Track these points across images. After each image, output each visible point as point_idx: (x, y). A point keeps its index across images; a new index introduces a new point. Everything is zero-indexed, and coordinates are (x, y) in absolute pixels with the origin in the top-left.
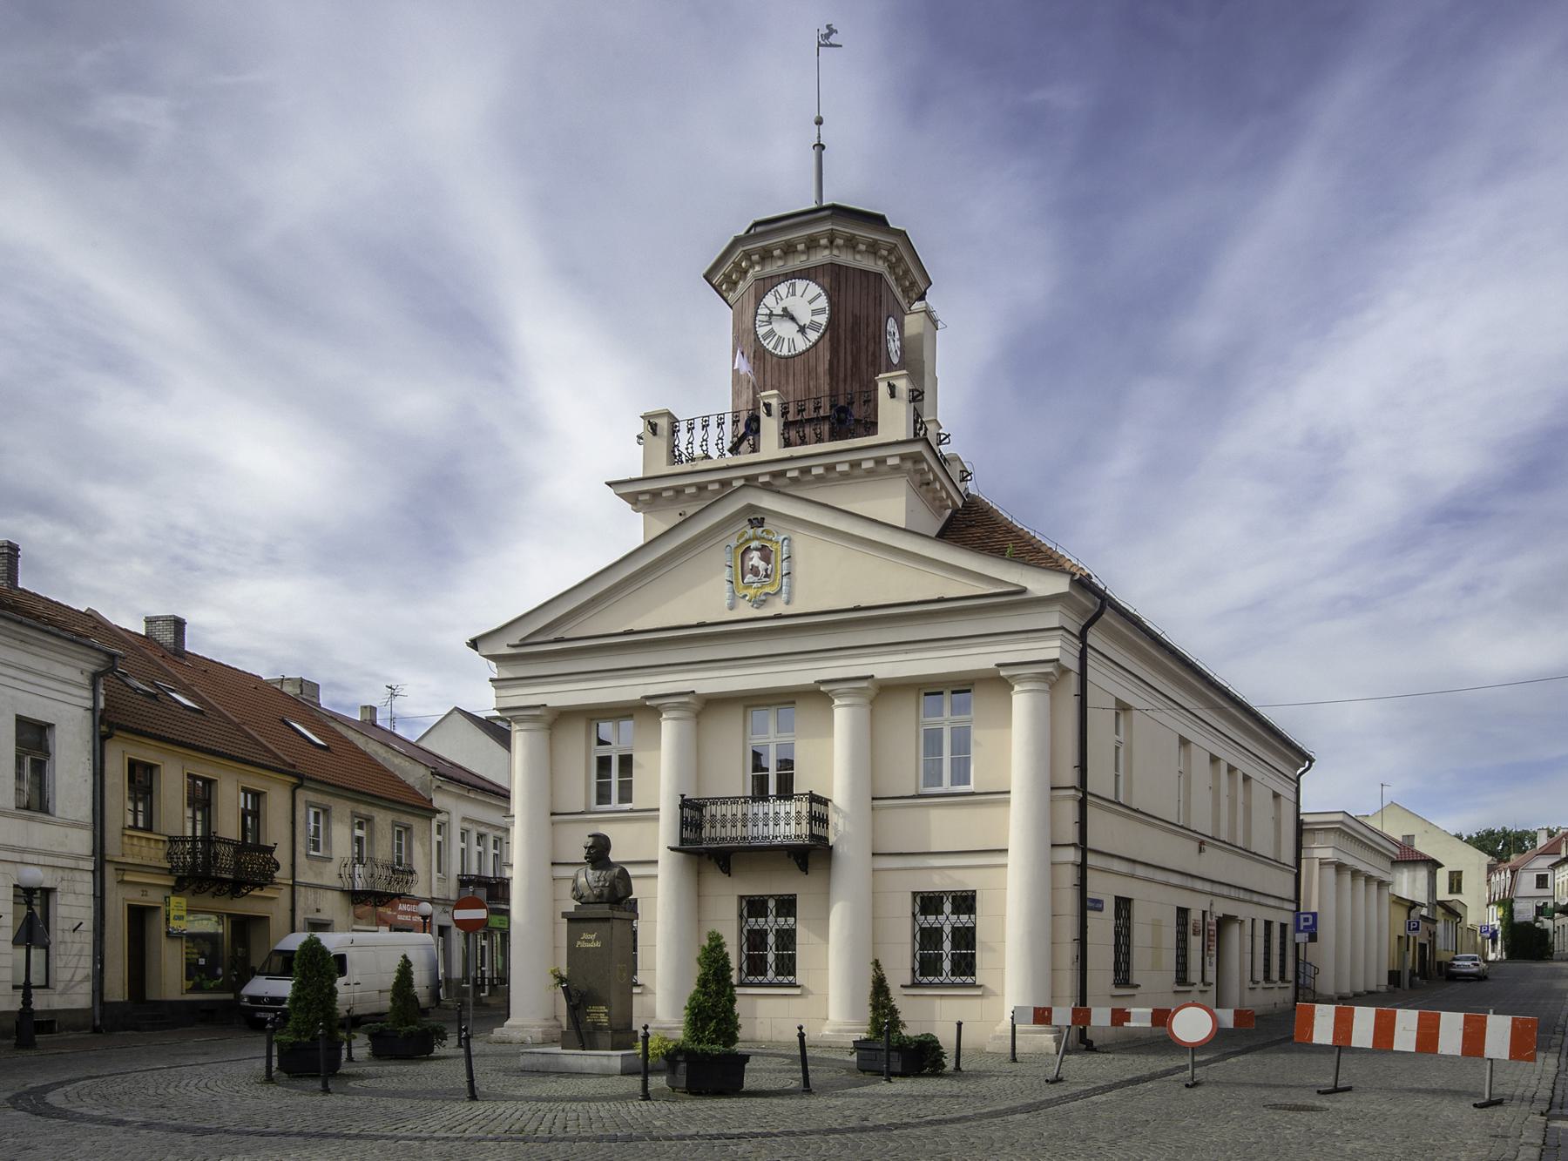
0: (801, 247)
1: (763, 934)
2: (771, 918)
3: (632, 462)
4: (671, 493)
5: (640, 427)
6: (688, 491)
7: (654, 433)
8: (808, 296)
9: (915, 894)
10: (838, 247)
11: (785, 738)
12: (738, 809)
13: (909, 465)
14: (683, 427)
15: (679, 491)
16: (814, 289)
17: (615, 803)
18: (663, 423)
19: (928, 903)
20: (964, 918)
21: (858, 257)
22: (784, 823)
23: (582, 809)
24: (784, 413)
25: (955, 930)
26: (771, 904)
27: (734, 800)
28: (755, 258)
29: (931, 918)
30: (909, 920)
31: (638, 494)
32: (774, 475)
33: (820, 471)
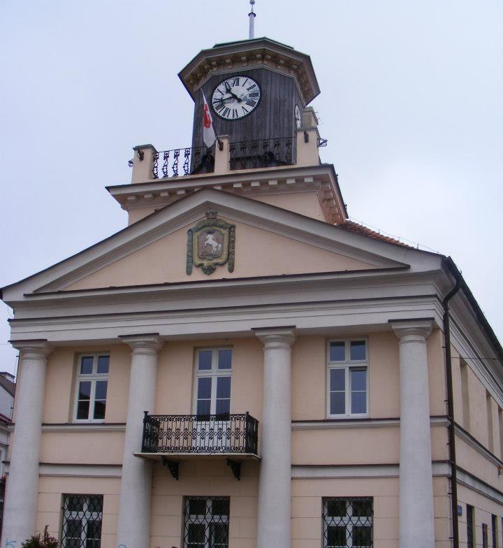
0: (244, 58)
2: (209, 516)
3: (125, 177)
4: (150, 196)
5: (132, 155)
6: (162, 195)
7: (141, 158)
8: (247, 85)
9: (324, 499)
10: (267, 59)
11: (224, 373)
12: (183, 425)
13: (319, 184)
14: (161, 156)
15: (156, 195)
16: (251, 82)
17: (91, 418)
18: (148, 154)
19: (334, 506)
20: (363, 519)
21: (279, 67)
22: (216, 439)
23: (66, 421)
24: (232, 149)
25: (355, 528)
26: (209, 504)
27: (179, 418)
28: (214, 63)
29: (337, 519)
30: (320, 521)
31: (124, 196)
32: (224, 186)
33: (257, 184)
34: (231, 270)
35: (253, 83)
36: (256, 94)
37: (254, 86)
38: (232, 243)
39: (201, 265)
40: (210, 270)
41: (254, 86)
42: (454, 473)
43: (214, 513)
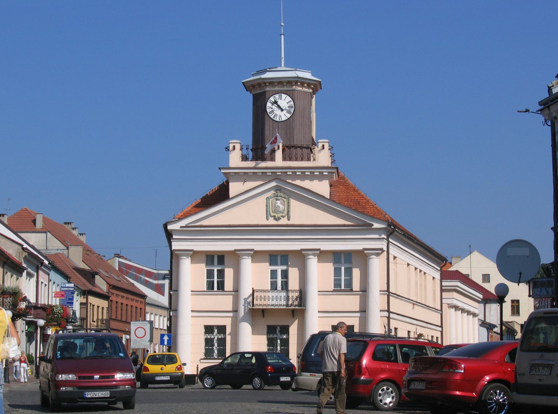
1: (212, 340)
16: (289, 99)
34: (289, 219)
35: (290, 99)
36: (292, 107)
37: (291, 101)
38: (289, 206)
39: (274, 216)
40: (279, 219)
41: (291, 101)
42: (389, 315)
43: (281, 334)
